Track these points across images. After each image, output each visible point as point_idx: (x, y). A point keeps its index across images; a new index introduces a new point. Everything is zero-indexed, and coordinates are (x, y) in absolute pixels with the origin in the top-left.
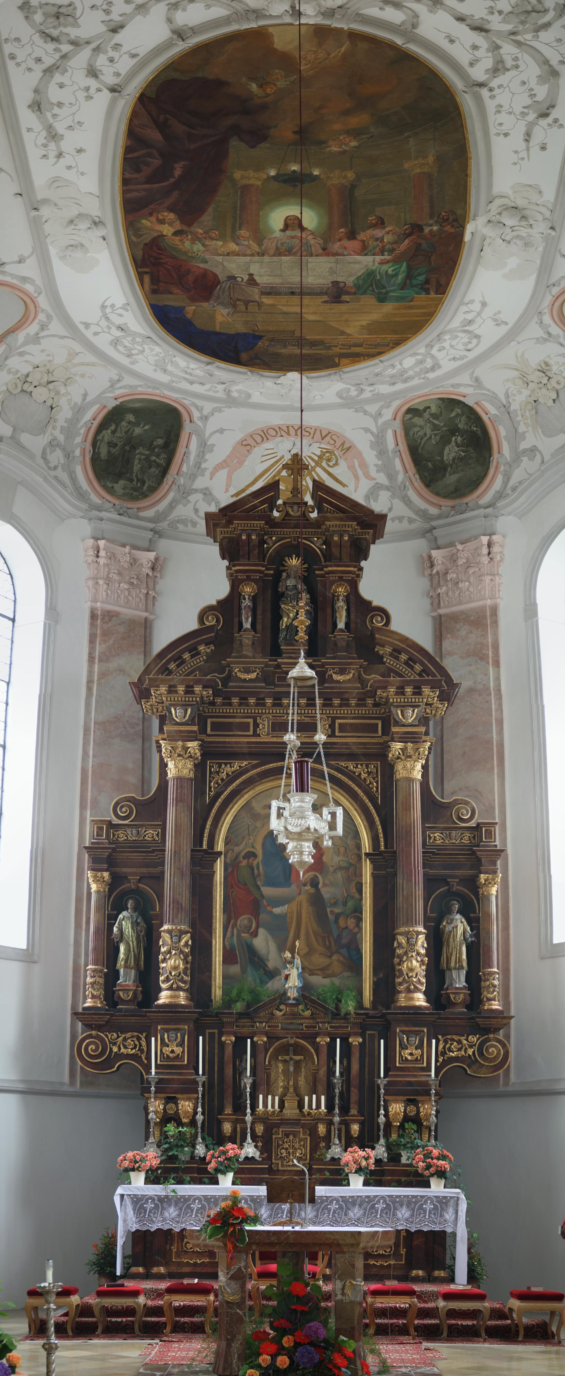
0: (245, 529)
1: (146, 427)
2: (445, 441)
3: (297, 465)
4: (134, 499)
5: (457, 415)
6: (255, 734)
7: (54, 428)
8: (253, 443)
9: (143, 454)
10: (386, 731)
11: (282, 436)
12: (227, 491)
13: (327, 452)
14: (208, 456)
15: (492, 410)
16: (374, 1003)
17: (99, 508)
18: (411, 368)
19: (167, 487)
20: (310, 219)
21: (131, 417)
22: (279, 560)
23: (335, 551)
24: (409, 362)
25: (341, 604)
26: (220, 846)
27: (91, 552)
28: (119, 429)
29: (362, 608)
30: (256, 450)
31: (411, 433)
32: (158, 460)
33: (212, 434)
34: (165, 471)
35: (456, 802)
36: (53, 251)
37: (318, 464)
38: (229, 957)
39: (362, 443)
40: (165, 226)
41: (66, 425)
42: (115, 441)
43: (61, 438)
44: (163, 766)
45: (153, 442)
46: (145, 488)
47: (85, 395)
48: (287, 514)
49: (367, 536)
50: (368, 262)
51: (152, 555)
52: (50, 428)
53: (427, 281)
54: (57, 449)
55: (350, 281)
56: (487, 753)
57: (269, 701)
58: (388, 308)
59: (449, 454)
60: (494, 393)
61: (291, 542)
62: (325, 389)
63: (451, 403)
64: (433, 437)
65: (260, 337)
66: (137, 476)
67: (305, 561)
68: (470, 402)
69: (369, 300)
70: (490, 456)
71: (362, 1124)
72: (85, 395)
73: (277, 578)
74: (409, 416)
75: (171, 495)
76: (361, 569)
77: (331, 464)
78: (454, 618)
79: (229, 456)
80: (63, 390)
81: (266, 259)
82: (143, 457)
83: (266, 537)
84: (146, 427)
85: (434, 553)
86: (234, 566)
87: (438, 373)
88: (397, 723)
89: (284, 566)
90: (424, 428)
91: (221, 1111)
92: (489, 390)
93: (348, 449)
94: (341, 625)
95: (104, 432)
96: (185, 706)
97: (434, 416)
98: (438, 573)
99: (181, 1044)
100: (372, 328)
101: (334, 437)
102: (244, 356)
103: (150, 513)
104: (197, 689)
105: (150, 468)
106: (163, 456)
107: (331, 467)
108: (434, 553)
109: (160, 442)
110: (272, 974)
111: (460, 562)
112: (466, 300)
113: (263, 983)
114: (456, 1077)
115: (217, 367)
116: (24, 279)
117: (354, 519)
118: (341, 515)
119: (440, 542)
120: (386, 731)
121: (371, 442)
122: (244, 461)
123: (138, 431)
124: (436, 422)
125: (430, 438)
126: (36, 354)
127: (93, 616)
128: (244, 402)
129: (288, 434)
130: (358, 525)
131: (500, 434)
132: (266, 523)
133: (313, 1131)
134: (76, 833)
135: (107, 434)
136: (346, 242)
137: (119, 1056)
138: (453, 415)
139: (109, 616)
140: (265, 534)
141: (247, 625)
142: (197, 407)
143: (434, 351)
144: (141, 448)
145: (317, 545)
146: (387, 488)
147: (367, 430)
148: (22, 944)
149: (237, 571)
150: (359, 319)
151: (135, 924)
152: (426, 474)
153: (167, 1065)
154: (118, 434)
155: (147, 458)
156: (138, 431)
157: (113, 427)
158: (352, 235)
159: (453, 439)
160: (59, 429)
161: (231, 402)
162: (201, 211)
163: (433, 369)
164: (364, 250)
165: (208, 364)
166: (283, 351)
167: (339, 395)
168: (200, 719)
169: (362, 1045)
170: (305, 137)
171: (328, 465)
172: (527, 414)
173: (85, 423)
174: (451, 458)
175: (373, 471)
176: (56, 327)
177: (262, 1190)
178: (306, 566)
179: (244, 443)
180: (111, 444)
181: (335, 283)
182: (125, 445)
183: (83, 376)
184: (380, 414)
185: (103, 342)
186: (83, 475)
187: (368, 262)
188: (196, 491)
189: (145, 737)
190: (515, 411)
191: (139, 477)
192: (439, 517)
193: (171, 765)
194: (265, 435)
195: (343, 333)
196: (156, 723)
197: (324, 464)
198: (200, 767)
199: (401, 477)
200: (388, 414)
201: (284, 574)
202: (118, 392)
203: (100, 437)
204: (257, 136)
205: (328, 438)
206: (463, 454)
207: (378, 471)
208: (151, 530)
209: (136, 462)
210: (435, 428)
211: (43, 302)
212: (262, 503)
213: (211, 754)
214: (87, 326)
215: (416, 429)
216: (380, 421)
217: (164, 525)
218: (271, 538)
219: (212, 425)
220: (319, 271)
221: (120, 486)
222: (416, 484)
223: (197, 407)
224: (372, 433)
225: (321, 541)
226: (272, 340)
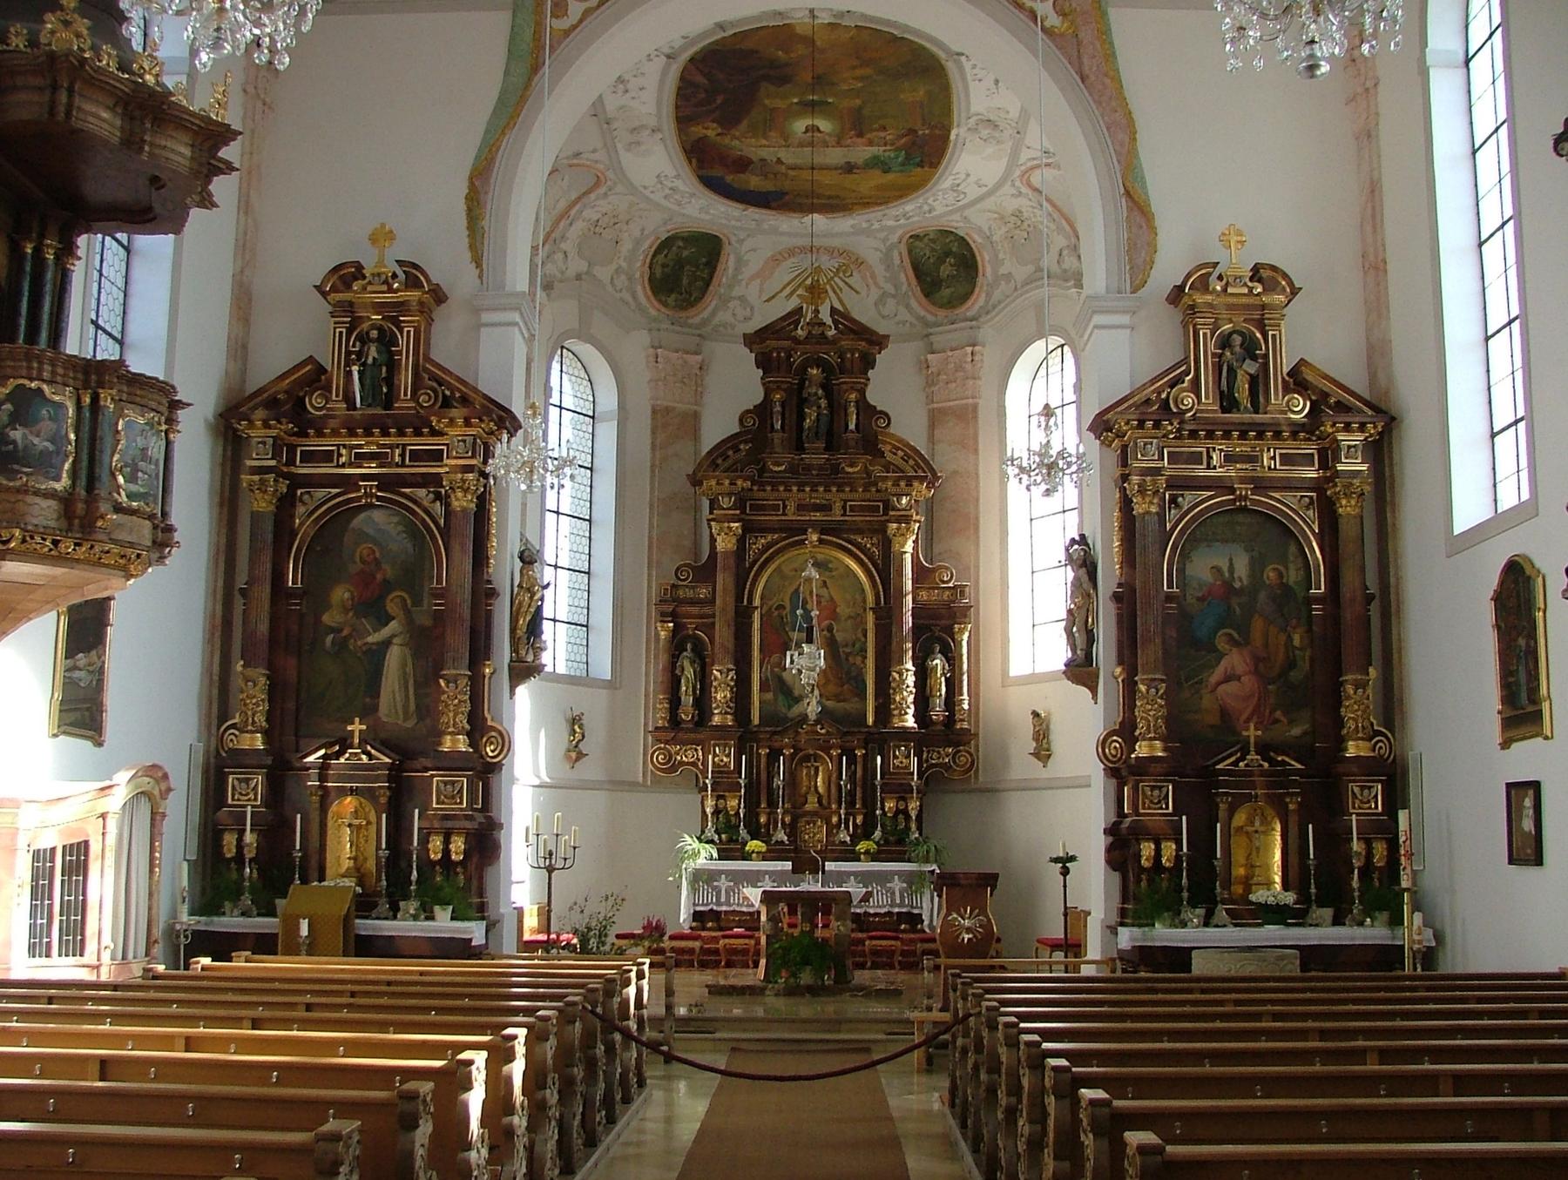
0: (772, 346)
2: (941, 260)
3: (815, 292)
4: (685, 309)
6: (784, 514)
10: (885, 514)
16: (875, 722)
17: (655, 320)
20: (824, 125)
21: (681, 244)
23: (848, 365)
24: (909, 207)
25: (852, 409)
26: (757, 602)
27: (652, 359)
29: (868, 412)
35: (940, 567)
36: (619, 146)
38: (764, 687)
39: (873, 258)
40: (711, 131)
43: (624, 265)
44: (713, 540)
50: (874, 150)
51: (699, 358)
55: (860, 162)
56: (969, 525)
57: (795, 489)
58: (890, 177)
69: (877, 172)
71: (865, 816)
73: (801, 386)
78: (943, 412)
85: (930, 357)
88: (895, 509)
91: (759, 804)
94: (852, 426)
96: (730, 495)
99: (728, 755)
100: (879, 188)
102: (773, 204)
103: (697, 320)
104: (739, 482)
110: (798, 700)
113: (790, 707)
114: (934, 779)
119: (935, 346)
120: (885, 514)
123: (685, 253)
126: (604, 206)
127: (654, 412)
131: (984, 258)
133: (828, 822)
134: (644, 591)
135: (660, 258)
137: (682, 763)
139: (668, 410)
141: (778, 426)
145: (832, 358)
146: (894, 296)
148: (607, 675)
150: (869, 182)
151: (692, 663)
153: (719, 771)
158: (860, 135)
162: (738, 121)
164: (871, 143)
168: (741, 503)
169: (865, 756)
170: (819, 81)
177: (788, 865)
180: (664, 266)
181: (848, 163)
186: (642, 292)
187: (874, 150)
189: (697, 509)
193: (719, 539)
194: (791, 252)
196: (706, 503)
198: (741, 541)
199: (904, 288)
200: (894, 238)
204: (783, 80)
210: (933, 250)
211: (610, 174)
213: (749, 528)
220: (835, 156)
221: (671, 300)
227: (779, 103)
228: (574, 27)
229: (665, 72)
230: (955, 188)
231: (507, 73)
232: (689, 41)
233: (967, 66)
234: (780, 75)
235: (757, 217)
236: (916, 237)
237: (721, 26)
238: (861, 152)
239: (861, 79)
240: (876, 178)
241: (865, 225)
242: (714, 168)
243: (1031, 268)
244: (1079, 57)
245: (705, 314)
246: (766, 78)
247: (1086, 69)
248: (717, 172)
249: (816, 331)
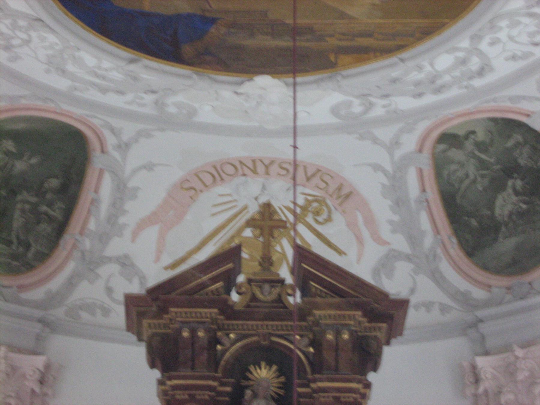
1: (34, 161)
2: (497, 186)
3: (267, 221)
5: (517, 145)
8: (199, 185)
9: (28, 202)
11: (244, 175)
12: (158, 259)
13: (315, 201)
14: (129, 206)
18: (448, 71)
19: (65, 254)
21: (9, 145)
22: (239, 370)
23: (328, 357)
24: (444, 61)
31: (445, 173)
32: (51, 212)
33: (135, 171)
34: (61, 228)
39: (370, 187)
46: (30, 255)
48: (254, 298)
49: (378, 334)
51: (39, 361)
59: (503, 206)
61: (258, 342)
64: (479, 179)
65: (213, 21)
66: (18, 237)
67: (281, 372)
74: (442, 147)
75: (71, 267)
76: (368, 386)
77: (320, 219)
82: (27, 206)
83: (219, 334)
84: (34, 161)
85: (481, 362)
86: (170, 379)
87: (489, 79)
89: (248, 379)
90: (465, 166)
93: (348, 196)
97: (479, 146)
98: (486, 392)
101: (327, 178)
102: (187, 50)
103: (37, 294)
105: (38, 222)
108: (481, 362)
109: (54, 183)
111: (521, 376)
115: (146, 67)
117: (358, 306)
118: (338, 300)
119: (490, 343)
121: (384, 186)
123: (20, 166)
125: (474, 181)
128: (187, 122)
129: (255, 172)
130: (365, 315)
132: (222, 312)
138: (510, 143)
140: (219, 329)
142: (113, 130)
143: (484, 46)
144: (25, 193)
145: (299, 346)
146: (408, 258)
147: (377, 167)
149: (175, 388)
152: (468, 237)
156: (20, 166)
159: (510, 183)
161: (164, 121)
163: (481, 73)
165: (132, 61)
166: (249, 42)
167: (335, 111)
171: (316, 221)
174: (506, 212)
175: (385, 231)
178: (282, 379)
184: (396, 143)
188: (110, 259)
191: (22, 237)
192: (487, 304)
194: (218, 172)
195: (343, 15)
197: (310, 219)
199: (429, 241)
200: (410, 143)
201: (248, 393)
205: (316, 180)
207: (394, 231)
208: (40, 321)
209: (17, 214)
210: (482, 165)
212: (214, 280)
215: (453, 167)
216: (398, 154)
217: (59, 313)
218: (228, 335)
219: (135, 158)
222: (451, 251)
223: (113, 130)
224: (384, 172)
225: (306, 341)
226: (233, 25)
236: (449, 139)
245: (56, 284)
249: (267, 295)
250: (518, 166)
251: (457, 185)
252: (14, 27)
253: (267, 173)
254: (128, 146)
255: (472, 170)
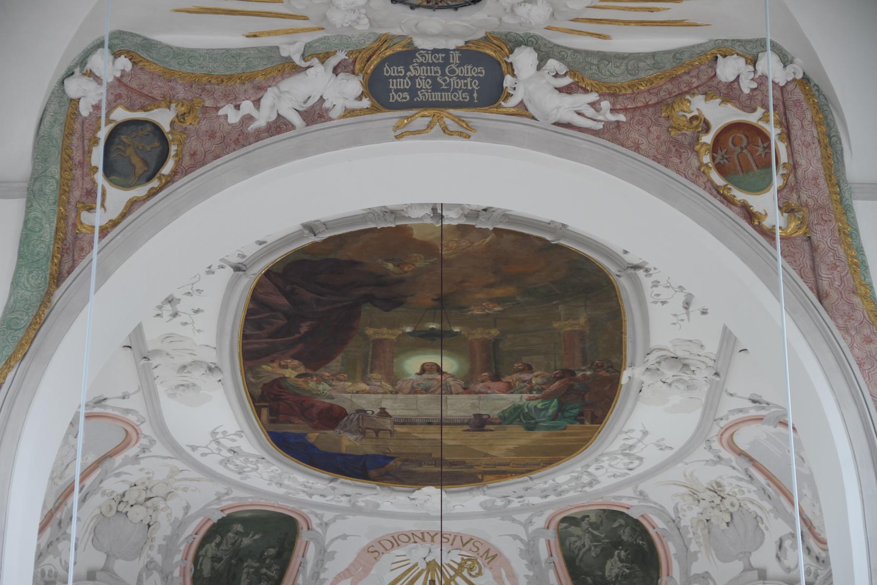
1: (256, 537)
2: (606, 554)
5: (621, 526)
7: (151, 548)
8: (381, 549)
9: (252, 567)
11: (415, 542)
13: (469, 560)
14: (328, 565)
15: (660, 524)
18: (565, 483)
20: (450, 365)
21: (239, 527)
28: (224, 541)
30: (386, 556)
31: (567, 543)
32: (269, 573)
36: (160, 389)
37: (458, 572)
39: (511, 551)
40: (290, 371)
41: (164, 543)
42: (219, 554)
43: (158, 558)
45: (263, 552)
47: (187, 508)
50: (515, 399)
52: (146, 549)
53: (581, 414)
54: (154, 572)
58: (537, 435)
59: (611, 569)
60: (661, 506)
62: (465, 508)
63: (612, 515)
64: (593, 548)
65: (392, 458)
68: (635, 514)
69: (516, 429)
70: (658, 577)
72: (187, 508)
74: (564, 525)
77: (473, 573)
79: (352, 564)
80: (162, 505)
81: (400, 396)
82: (252, 570)
84: (256, 537)
87: (597, 487)
90: (581, 538)
92: (655, 503)
95: (208, 546)
97: (591, 524)
100: (519, 451)
102: (373, 473)
106: (275, 567)
107: (474, 576)
109: (272, 551)
112: (625, 429)
115: (342, 483)
116: (127, 411)
121: (521, 550)
122: (370, 569)
123: (246, 541)
124: (596, 533)
125: (590, 549)
126: (134, 473)
128: (374, 511)
129: (423, 540)
131: (669, 550)
136: (489, 383)
138: (615, 525)
142: (316, 515)
144: (249, 560)
147: (516, 537)
150: (504, 444)
154: (224, 547)
155: (257, 570)
156: (246, 541)
157: (218, 540)
158: (496, 378)
159: (616, 553)
160: (156, 548)
161: (355, 510)
162: (329, 358)
163: (590, 484)
164: (510, 388)
165: (331, 481)
166: (418, 469)
170: (444, 304)
171: (470, 575)
172: (699, 532)
173: (187, 538)
174: (614, 575)
176: (158, 449)
179: (371, 549)
180: (215, 559)
182: (231, 558)
183: (185, 490)
184: (530, 522)
185: (212, 462)
187: (515, 399)
190: (686, 527)
194: (395, 541)
195: (486, 455)
197: (465, 573)
200: (540, 522)
202: (224, 504)
203: (202, 552)
204: (392, 302)
205: (470, 545)
206: (628, 571)
209: (244, 576)
210: (595, 538)
211: (145, 429)
214: (194, 448)
215: (573, 539)
216: (531, 529)
219: (333, 531)
220: (460, 406)
223: (316, 515)
224: (521, 540)
226: (406, 460)
227: (386, 333)
228: (114, 224)
229: (232, 286)
230: (627, 451)
231: (15, 283)
232: (266, 248)
233: (647, 282)
234: (389, 295)
235: (349, 490)
236: (570, 520)
237: (310, 228)
238: (498, 401)
239: (498, 301)
240: (518, 438)
241: (499, 503)
242: (291, 422)
243: (737, 566)
244: (814, 269)
246: (370, 299)
247: (825, 285)
248: (294, 427)
250: (622, 540)
251: (576, 552)
252: (246, 461)
253: (433, 541)
254: (327, 524)
255: (588, 543)
